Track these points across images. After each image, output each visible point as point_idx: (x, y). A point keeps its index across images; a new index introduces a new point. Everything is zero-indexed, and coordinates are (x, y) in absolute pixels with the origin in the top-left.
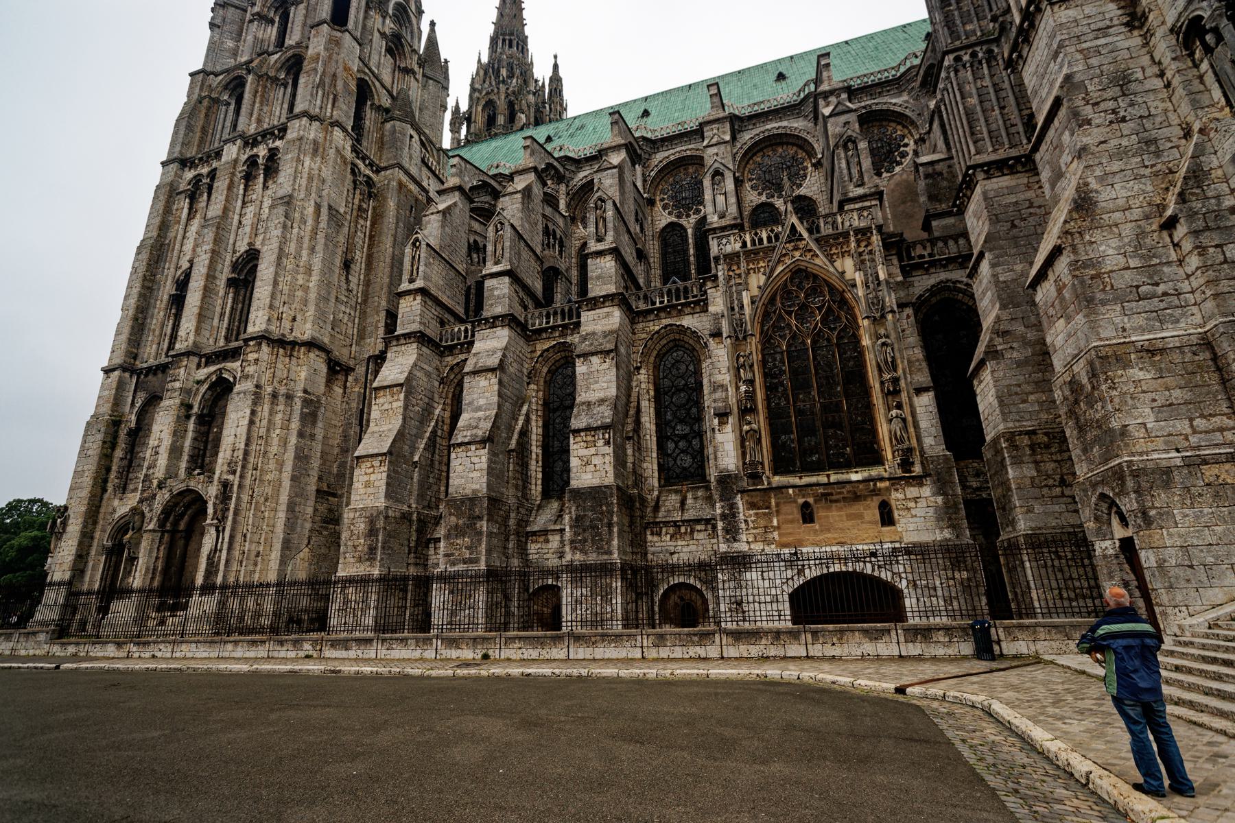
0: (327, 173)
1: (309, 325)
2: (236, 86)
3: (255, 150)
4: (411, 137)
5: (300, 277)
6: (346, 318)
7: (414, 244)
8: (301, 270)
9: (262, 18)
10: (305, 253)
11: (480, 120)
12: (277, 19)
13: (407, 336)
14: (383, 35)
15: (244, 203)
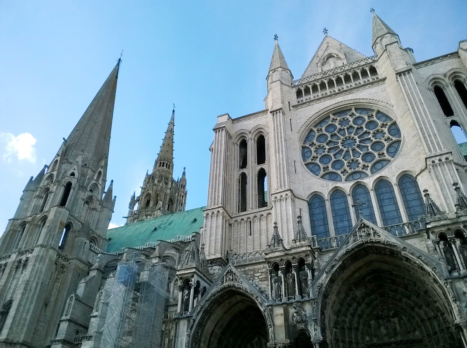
0: (44, 270)
1: (23, 336)
2: (23, 225)
3: (22, 257)
4: (86, 243)
5: (24, 314)
6: (42, 328)
7: (71, 298)
8: (26, 311)
9: (39, 197)
10: (28, 303)
11: (143, 202)
12: (44, 196)
13: (59, 341)
14: (83, 199)
15: (13, 278)
